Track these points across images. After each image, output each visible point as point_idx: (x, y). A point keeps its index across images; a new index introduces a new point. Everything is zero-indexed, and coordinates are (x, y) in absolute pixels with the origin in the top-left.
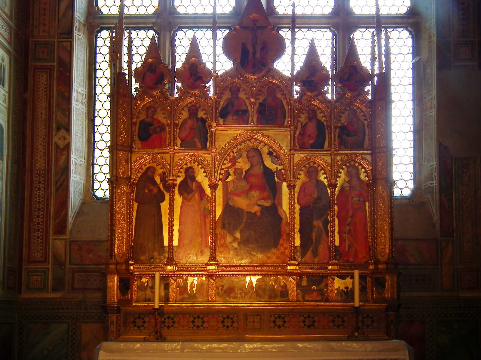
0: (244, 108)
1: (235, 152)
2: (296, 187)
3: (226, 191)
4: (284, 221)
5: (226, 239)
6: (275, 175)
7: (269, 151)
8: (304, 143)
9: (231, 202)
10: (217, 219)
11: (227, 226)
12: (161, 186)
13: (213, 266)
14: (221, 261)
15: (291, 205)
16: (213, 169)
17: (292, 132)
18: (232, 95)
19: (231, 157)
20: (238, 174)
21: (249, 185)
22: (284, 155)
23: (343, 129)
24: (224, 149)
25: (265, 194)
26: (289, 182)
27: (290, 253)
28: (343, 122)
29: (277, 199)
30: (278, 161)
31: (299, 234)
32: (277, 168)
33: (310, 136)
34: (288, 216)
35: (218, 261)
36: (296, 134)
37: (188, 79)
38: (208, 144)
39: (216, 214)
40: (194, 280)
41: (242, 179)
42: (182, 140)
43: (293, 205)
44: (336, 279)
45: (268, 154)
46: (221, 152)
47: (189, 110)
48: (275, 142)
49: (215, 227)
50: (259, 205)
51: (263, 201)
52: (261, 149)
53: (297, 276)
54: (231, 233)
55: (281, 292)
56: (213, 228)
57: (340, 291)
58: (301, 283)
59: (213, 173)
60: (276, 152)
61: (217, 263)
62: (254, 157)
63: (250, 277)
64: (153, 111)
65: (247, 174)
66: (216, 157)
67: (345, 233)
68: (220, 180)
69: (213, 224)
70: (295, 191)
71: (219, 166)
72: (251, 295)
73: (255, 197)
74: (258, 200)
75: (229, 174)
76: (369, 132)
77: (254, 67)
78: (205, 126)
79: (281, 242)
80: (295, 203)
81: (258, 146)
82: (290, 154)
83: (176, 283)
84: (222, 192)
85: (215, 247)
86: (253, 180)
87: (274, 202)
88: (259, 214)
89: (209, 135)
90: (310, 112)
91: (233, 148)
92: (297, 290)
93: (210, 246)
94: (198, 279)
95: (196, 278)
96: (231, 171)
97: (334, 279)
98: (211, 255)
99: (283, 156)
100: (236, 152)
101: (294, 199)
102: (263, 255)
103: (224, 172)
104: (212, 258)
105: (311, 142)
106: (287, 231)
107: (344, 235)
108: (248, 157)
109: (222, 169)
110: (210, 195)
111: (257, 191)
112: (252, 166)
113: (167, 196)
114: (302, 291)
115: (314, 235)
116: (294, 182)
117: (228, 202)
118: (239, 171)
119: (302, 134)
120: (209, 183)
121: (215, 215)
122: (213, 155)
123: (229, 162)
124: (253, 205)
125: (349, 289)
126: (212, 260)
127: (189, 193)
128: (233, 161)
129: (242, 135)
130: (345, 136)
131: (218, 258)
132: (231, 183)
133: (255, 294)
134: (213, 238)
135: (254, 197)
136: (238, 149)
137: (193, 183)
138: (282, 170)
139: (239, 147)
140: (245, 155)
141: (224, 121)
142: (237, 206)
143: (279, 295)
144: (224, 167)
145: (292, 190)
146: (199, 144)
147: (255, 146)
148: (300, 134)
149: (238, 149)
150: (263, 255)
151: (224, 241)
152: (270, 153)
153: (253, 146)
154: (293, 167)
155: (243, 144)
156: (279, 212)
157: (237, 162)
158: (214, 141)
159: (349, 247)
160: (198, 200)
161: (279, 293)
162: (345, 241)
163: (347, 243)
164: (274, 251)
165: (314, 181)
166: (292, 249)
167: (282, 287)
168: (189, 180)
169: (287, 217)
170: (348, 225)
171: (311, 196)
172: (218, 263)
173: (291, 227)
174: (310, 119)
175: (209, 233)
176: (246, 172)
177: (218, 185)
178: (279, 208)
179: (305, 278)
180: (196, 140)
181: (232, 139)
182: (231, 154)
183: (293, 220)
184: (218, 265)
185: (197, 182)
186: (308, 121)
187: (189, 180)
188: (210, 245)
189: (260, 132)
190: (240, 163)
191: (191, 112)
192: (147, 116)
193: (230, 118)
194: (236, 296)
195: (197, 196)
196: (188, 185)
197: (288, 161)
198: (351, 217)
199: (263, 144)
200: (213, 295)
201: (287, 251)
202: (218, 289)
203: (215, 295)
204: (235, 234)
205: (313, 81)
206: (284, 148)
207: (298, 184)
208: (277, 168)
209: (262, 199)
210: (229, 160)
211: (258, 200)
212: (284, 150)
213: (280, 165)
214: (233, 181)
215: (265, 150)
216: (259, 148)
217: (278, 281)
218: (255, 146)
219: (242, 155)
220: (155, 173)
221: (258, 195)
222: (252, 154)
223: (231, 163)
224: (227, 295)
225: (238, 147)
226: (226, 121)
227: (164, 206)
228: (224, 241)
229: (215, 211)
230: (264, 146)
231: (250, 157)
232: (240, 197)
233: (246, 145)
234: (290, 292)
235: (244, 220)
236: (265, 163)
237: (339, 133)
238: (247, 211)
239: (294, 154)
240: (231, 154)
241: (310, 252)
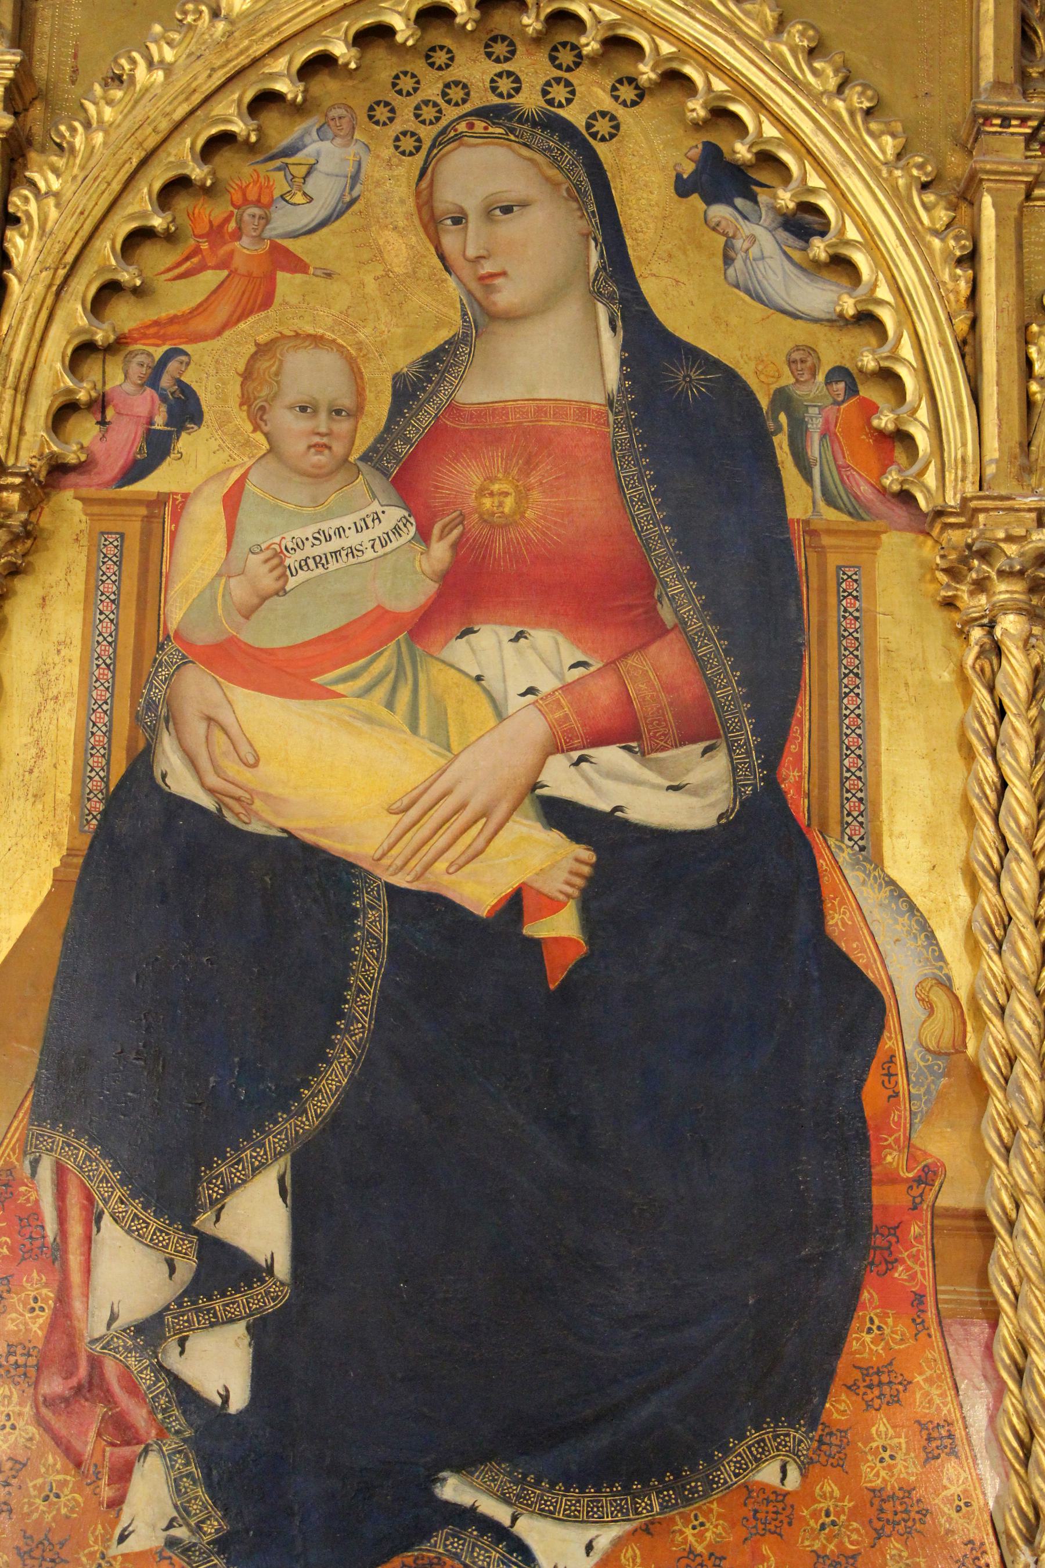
3: (129, 615)
5: (87, 1270)
6: (781, 443)
21: (440, 551)
45: (683, 188)
51: (611, 755)
52: (603, 126)
62: (507, 210)
65: (424, 420)
73: (515, 703)
74: (557, 746)
81: (559, 93)
87: (772, 785)
102: (606, 1536)
111: (542, 637)
124: (485, 813)
135: (500, 715)
151: (63, 1297)
153: (505, 85)
156: (836, 921)
157: (297, 265)
164: (768, 1474)
211: (557, 746)
216: (575, 115)
221: (547, 684)
228: (63, 1297)
232: (325, 693)
236: (649, 288)
238: (401, 881)
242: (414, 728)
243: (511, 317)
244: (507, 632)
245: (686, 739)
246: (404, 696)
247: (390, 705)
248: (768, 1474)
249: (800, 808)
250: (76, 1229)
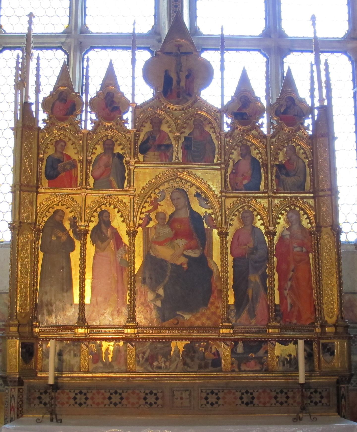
0: (167, 142)
1: (157, 193)
2: (228, 235)
4: (215, 274)
6: (204, 221)
7: (197, 193)
8: (237, 184)
9: (153, 252)
10: (136, 272)
11: (148, 281)
12: (71, 233)
13: (132, 328)
14: (141, 322)
15: (223, 256)
16: (132, 214)
17: (223, 171)
18: (153, 128)
19: (153, 199)
20: (161, 219)
21: (174, 232)
22: (214, 198)
23: (281, 167)
24: (144, 189)
25: (193, 243)
26: (221, 229)
27: (222, 312)
28: (280, 160)
29: (206, 249)
30: (207, 204)
31: (232, 290)
32: (206, 212)
33: (243, 175)
34: (220, 269)
35: (137, 323)
36: (227, 173)
37: (104, 110)
38: (126, 183)
39: (135, 266)
40: (109, 345)
41: (164, 225)
42: (95, 179)
43: (226, 256)
44: (278, 344)
45: (195, 196)
46: (141, 193)
47: (104, 145)
48: (203, 182)
49: (134, 281)
50: (185, 256)
51: (189, 250)
52: (187, 190)
53: (232, 341)
54: (154, 289)
55: (213, 360)
56: (131, 284)
57: (282, 359)
58: (236, 350)
59: (132, 218)
60: (204, 193)
61: (136, 324)
62: (179, 199)
63: (176, 343)
64: (62, 146)
66: (135, 199)
67: (286, 290)
68: (140, 225)
69: (131, 277)
70: (228, 239)
71: (138, 210)
72: (177, 365)
73: (181, 246)
74: (184, 250)
75: (150, 219)
76: (310, 171)
77: (178, 96)
78: (122, 163)
79: (211, 300)
80: (227, 254)
82: (221, 197)
83: (89, 350)
84: (141, 240)
85: (134, 306)
86: (178, 226)
88: (185, 266)
89: (127, 173)
90: (243, 148)
91: (155, 189)
92: (231, 358)
93: (128, 305)
94: (114, 344)
95: (112, 343)
96: (153, 215)
97: (274, 345)
98: (130, 315)
99: (213, 198)
100: (159, 193)
101: (227, 249)
102: (190, 316)
103: (144, 216)
104: (130, 319)
105: (245, 182)
106: (219, 288)
107: (285, 292)
108: (172, 200)
109: (142, 213)
110: (128, 244)
111: (183, 240)
112: (177, 209)
113: (78, 244)
114: (237, 359)
115: (250, 292)
116: (227, 229)
117: (148, 252)
118: (161, 216)
119: (235, 173)
120: (127, 229)
121: (134, 267)
122: (132, 197)
123: (150, 205)
125: (292, 357)
126: (130, 322)
127: (103, 241)
128: (155, 204)
129: (165, 173)
130: (283, 175)
131: (137, 319)
132: (153, 229)
133: (182, 363)
134: (131, 295)
135: (179, 246)
136: (161, 189)
137: (108, 230)
138: (212, 214)
139: (161, 188)
140: (168, 196)
141: (143, 158)
142: (159, 257)
143: (210, 365)
144: (144, 210)
145: (224, 238)
146: (115, 184)
147: (181, 186)
148: (232, 172)
149: (161, 189)
150: (190, 316)
152: (198, 195)
154: (225, 211)
155: (166, 184)
156: (209, 265)
157: (160, 205)
158: (132, 181)
159: (292, 306)
160: (113, 250)
161: (210, 362)
162: (286, 299)
163: (289, 301)
164: (203, 311)
165: (249, 227)
166: (224, 309)
167: (214, 354)
168: (103, 226)
169: (218, 270)
170: (290, 280)
171: (246, 245)
172: (137, 325)
173: (224, 283)
174: (243, 156)
175: (126, 288)
176: (171, 216)
177: (138, 232)
178: (209, 259)
179: (240, 344)
180: (112, 178)
181: (153, 178)
182: (153, 195)
183: (226, 273)
184: (138, 327)
185: (113, 228)
186: (240, 158)
187: (103, 226)
188: (128, 303)
189: (186, 170)
190: (162, 206)
191: (106, 146)
192: (56, 151)
193: (150, 154)
194: (160, 365)
195: (112, 244)
196: (102, 233)
197: (219, 204)
198: (293, 271)
199: (189, 184)
200: (133, 364)
201: (218, 310)
202: (139, 358)
203: (134, 365)
204: (157, 291)
205: (246, 114)
206: (213, 189)
207: (231, 231)
208: (206, 212)
209: (188, 249)
210: (150, 203)
211: (184, 250)
212: (214, 191)
213: (209, 209)
214: (155, 227)
215: (192, 191)
217: (210, 348)
218: (181, 186)
219: (165, 196)
220: (63, 217)
221: (184, 244)
222: (177, 195)
223: (152, 206)
224: (148, 363)
225: (160, 187)
226: (147, 157)
227: (75, 256)
229: (134, 263)
230: (191, 187)
231: (174, 200)
233: (170, 184)
234: (223, 361)
235: (168, 274)
236: (192, 206)
237: (276, 172)
238: (172, 262)
239: (226, 197)
240: (153, 195)
241: (246, 312)
242: (172, 248)
243: (179, 209)
244: (180, 239)
245: (196, 249)
246: (171, 246)
247: (170, 246)
248: (203, 311)
249: (206, 255)
250: (146, 293)
